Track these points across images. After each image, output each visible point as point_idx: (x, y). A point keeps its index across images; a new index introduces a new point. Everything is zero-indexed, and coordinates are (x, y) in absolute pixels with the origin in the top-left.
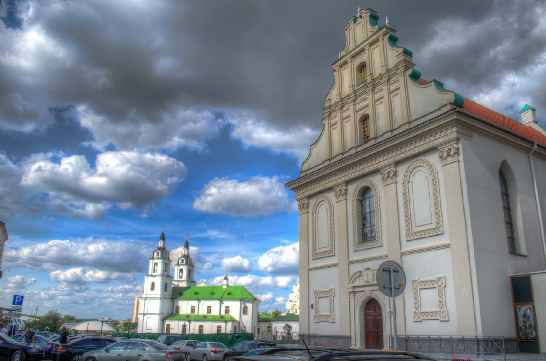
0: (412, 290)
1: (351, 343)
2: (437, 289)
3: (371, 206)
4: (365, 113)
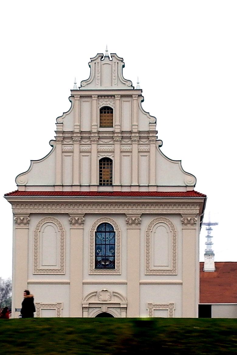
0: (147, 310)
2: (169, 311)
3: (106, 240)
4: (107, 157)
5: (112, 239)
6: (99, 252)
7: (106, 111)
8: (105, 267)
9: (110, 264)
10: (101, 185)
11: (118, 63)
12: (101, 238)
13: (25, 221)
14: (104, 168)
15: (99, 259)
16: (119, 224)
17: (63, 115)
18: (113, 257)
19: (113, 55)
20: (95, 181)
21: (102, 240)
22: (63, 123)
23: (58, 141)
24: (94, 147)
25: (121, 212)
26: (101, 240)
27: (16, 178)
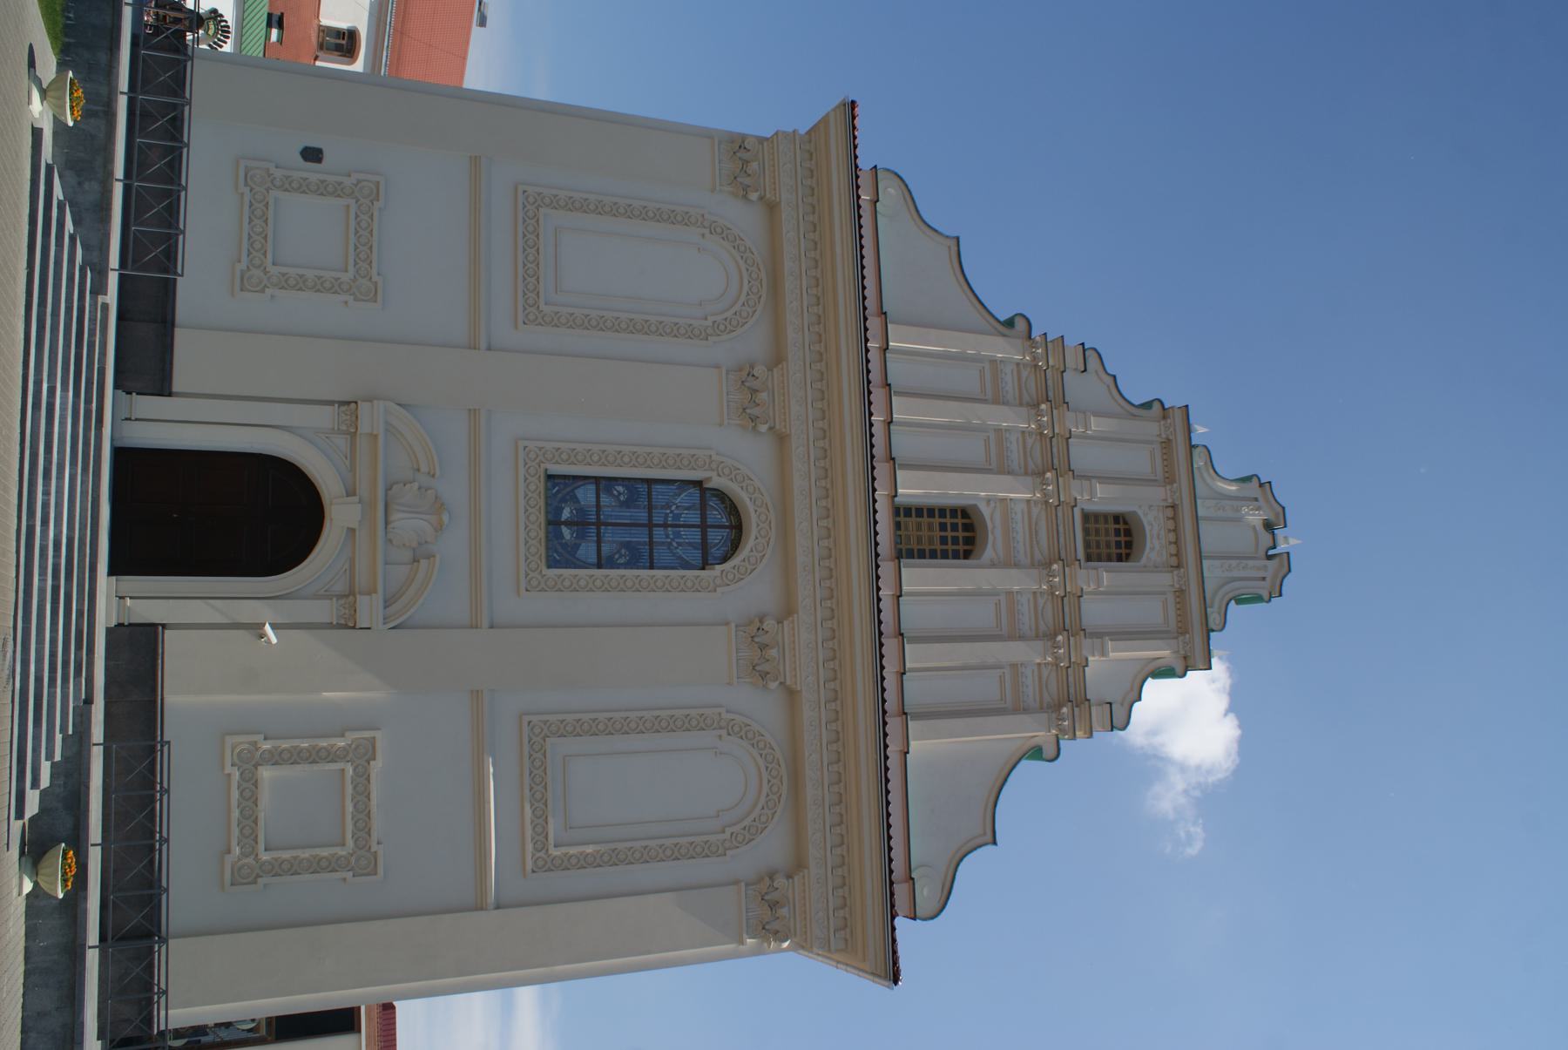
1: (138, 394)
4: (990, 537)
5: (674, 554)
6: (617, 497)
8: (554, 523)
9: (565, 546)
11: (1264, 579)
12: (677, 507)
14: (943, 527)
15: (587, 495)
17: (1109, 374)
18: (594, 559)
21: (668, 511)
22: (1084, 373)
26: (669, 507)
27: (896, 174)
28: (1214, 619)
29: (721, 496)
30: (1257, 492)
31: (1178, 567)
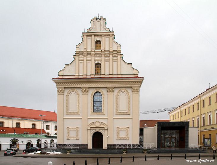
7: (98, 42)
8: (98, 112)
10: (96, 75)
13: (62, 91)
14: (97, 68)
15: (95, 108)
16: (104, 92)
19: (101, 17)
20: (93, 72)
23: (77, 55)
24: (93, 58)
25: (104, 86)
28: (108, 30)
29: (95, 94)
30: (93, 21)
31: (102, 35)
